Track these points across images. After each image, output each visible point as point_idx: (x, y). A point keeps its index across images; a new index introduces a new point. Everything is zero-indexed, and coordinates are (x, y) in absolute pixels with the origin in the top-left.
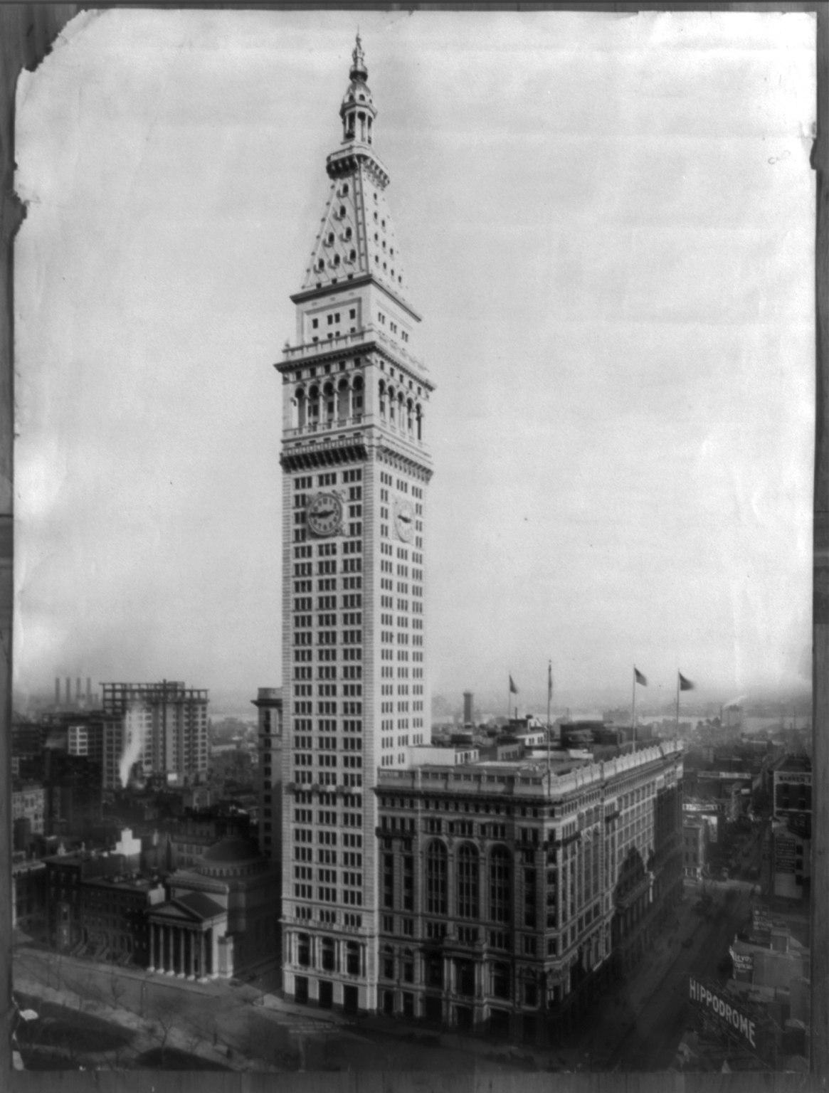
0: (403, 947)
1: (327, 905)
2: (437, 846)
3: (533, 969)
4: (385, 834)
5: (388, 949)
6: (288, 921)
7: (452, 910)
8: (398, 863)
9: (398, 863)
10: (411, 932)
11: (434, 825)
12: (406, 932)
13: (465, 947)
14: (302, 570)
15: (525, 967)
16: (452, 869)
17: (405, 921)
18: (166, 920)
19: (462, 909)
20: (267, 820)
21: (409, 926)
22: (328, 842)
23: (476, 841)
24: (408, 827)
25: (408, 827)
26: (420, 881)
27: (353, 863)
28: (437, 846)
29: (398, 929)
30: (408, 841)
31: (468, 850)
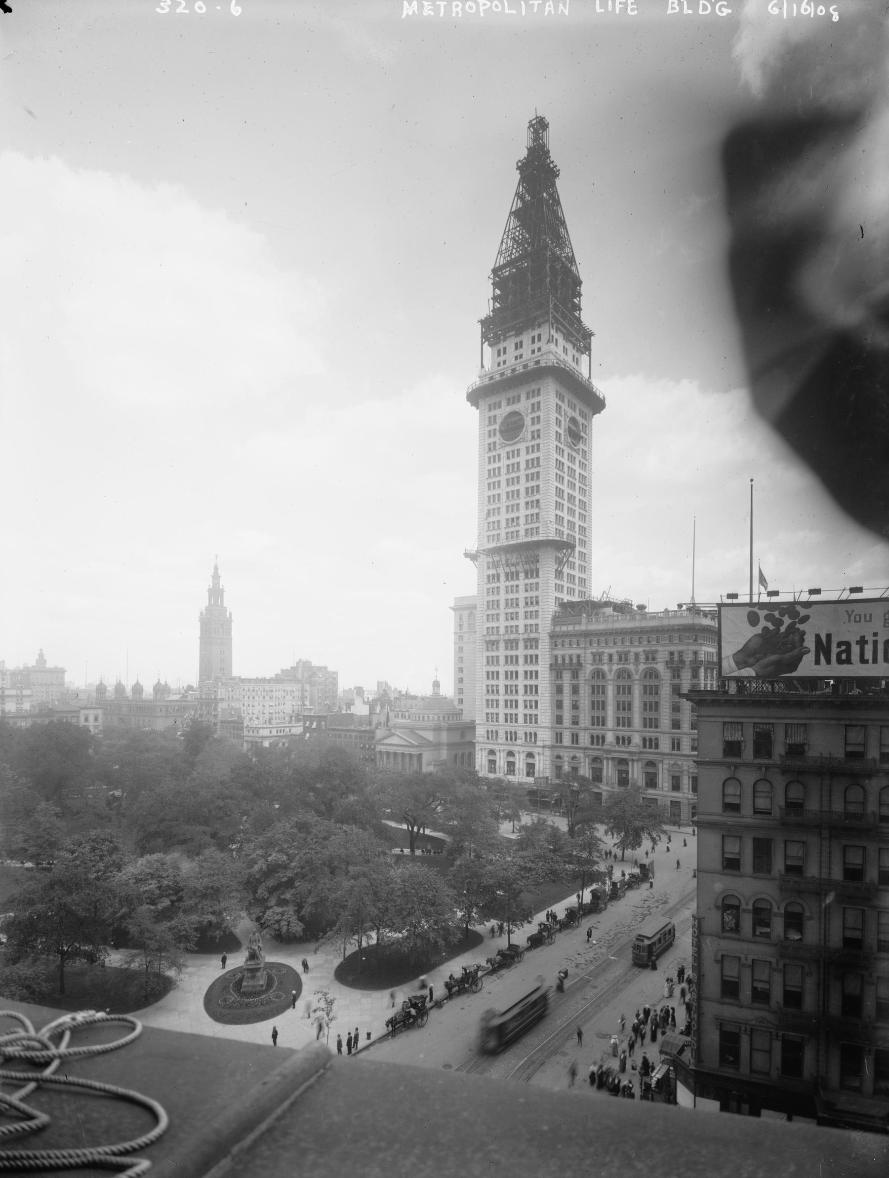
0: (571, 755)
1: (511, 727)
2: (599, 674)
3: (679, 763)
4: (557, 669)
5: (559, 757)
6: (481, 739)
7: (610, 722)
8: (567, 690)
9: (567, 690)
10: (577, 743)
11: (597, 658)
12: (573, 743)
13: (622, 749)
14: (492, 499)
15: (672, 762)
16: (611, 691)
17: (573, 735)
18: (388, 747)
19: (619, 722)
20: (461, 697)
21: (575, 738)
22: (512, 678)
23: (631, 667)
24: (575, 661)
25: (575, 661)
26: (585, 701)
27: (531, 693)
28: (599, 674)
29: (567, 740)
30: (575, 675)
31: (623, 674)
